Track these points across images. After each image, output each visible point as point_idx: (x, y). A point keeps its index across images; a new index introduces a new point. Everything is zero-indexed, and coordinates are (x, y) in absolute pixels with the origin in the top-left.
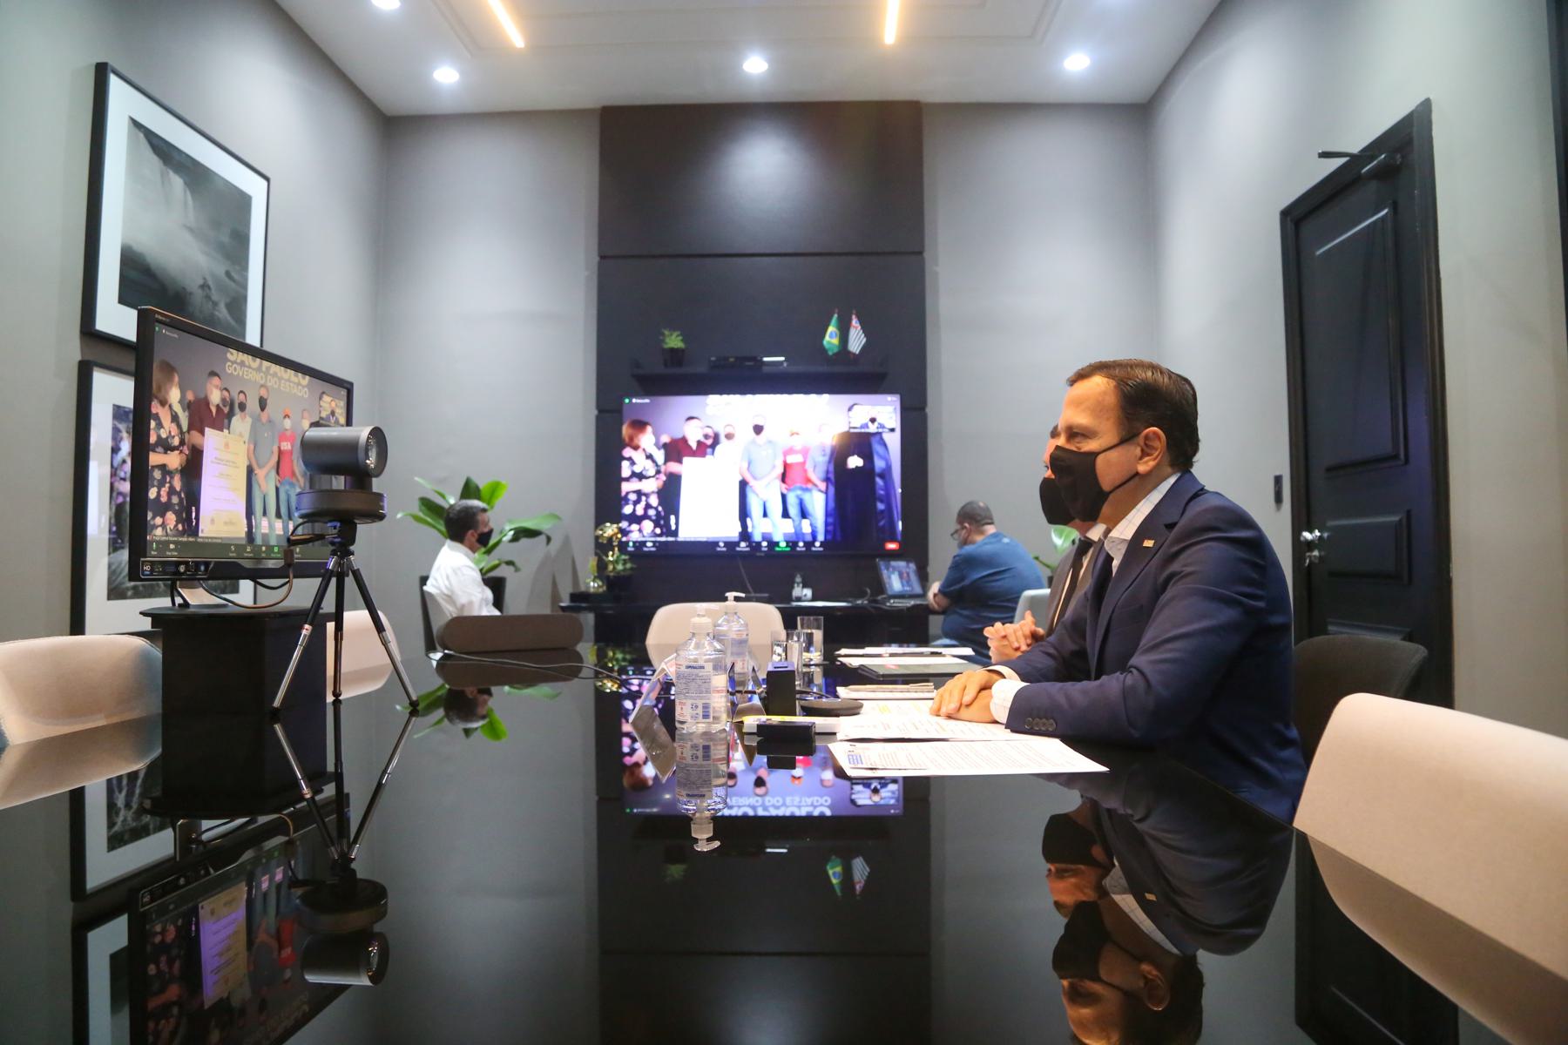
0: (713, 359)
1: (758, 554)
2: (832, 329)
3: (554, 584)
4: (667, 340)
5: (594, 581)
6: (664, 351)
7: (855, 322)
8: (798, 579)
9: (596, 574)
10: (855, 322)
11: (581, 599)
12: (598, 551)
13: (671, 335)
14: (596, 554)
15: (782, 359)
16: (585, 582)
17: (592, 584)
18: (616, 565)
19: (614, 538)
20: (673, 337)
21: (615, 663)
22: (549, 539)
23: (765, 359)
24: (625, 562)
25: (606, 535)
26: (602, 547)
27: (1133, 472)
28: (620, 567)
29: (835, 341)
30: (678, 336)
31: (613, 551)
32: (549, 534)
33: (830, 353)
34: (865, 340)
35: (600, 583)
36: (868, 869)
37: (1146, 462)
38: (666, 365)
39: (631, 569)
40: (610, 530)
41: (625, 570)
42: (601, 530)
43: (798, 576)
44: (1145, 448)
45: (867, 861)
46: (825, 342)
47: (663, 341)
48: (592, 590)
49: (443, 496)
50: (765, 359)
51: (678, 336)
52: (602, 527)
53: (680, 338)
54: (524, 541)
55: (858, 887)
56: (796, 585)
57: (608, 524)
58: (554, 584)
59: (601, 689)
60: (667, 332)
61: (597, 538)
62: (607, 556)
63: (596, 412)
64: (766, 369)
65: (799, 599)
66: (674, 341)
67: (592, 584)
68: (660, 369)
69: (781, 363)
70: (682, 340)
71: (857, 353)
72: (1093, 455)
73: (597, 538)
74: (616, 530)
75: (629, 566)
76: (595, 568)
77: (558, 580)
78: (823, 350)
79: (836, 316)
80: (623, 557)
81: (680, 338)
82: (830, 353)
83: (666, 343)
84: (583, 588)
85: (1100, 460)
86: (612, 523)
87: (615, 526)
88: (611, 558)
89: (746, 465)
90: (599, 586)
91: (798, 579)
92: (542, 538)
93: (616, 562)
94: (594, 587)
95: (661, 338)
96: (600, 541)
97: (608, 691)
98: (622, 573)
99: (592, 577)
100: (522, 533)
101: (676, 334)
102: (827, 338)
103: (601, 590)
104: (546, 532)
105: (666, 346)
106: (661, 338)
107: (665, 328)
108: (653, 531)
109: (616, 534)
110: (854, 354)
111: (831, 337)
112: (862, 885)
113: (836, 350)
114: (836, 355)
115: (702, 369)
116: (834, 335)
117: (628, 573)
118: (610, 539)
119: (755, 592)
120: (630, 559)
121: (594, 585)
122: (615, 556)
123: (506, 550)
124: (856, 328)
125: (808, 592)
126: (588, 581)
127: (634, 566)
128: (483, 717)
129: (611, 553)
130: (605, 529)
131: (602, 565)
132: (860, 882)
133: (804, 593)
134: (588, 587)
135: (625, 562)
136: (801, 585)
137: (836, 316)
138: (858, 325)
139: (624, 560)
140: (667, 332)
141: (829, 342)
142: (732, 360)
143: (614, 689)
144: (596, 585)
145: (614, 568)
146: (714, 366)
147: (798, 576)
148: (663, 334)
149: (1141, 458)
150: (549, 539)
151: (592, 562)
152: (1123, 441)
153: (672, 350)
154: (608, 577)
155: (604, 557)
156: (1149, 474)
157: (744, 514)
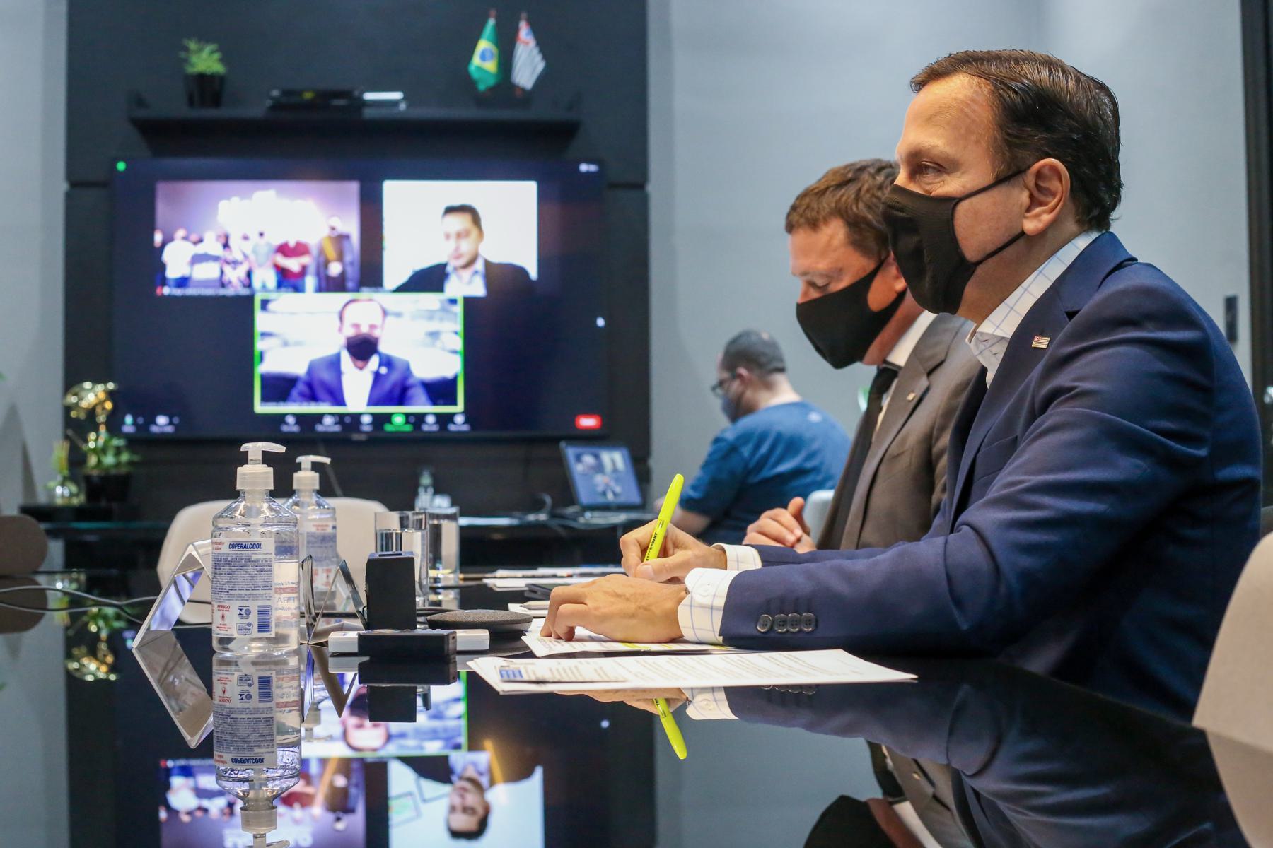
1: (356, 437)
2: (484, 45)
4: (194, 59)
5: (63, 485)
7: (524, 32)
9: (66, 472)
10: (524, 32)
12: (70, 432)
14: (67, 437)
16: (45, 487)
17: (59, 490)
21: (101, 623)
23: (369, 96)
24: (118, 451)
25: (84, 404)
29: (491, 66)
30: (212, 52)
31: (97, 430)
33: (482, 87)
39: (131, 463)
41: (118, 465)
48: (59, 502)
50: (369, 96)
52: (76, 389)
57: (87, 385)
59: (77, 675)
60: (193, 45)
61: (68, 409)
62: (86, 441)
64: (368, 113)
66: (206, 61)
67: (59, 490)
73: (68, 409)
76: (65, 463)
78: (469, 82)
79: (491, 23)
80: (117, 442)
81: (217, 56)
82: (482, 87)
83: (193, 65)
84: (42, 499)
86: (96, 381)
88: (92, 445)
90: (72, 495)
93: (102, 451)
96: (73, 414)
97: (90, 678)
98: (113, 472)
99: (60, 478)
102: (476, 60)
103: (75, 501)
107: (189, 38)
109: (102, 403)
110: (523, 90)
111: (483, 57)
113: (491, 82)
114: (492, 89)
116: (488, 54)
117: (124, 470)
121: (62, 493)
122: (101, 441)
124: (527, 43)
126: (51, 484)
127: (136, 458)
129: (92, 436)
130: (83, 394)
131: (76, 459)
134: (51, 493)
135: (118, 451)
137: (491, 23)
140: (193, 45)
141: (479, 69)
143: (102, 675)
144: (67, 493)
145: (99, 462)
151: (60, 451)
153: (202, 78)
154: (88, 479)
155: (79, 443)
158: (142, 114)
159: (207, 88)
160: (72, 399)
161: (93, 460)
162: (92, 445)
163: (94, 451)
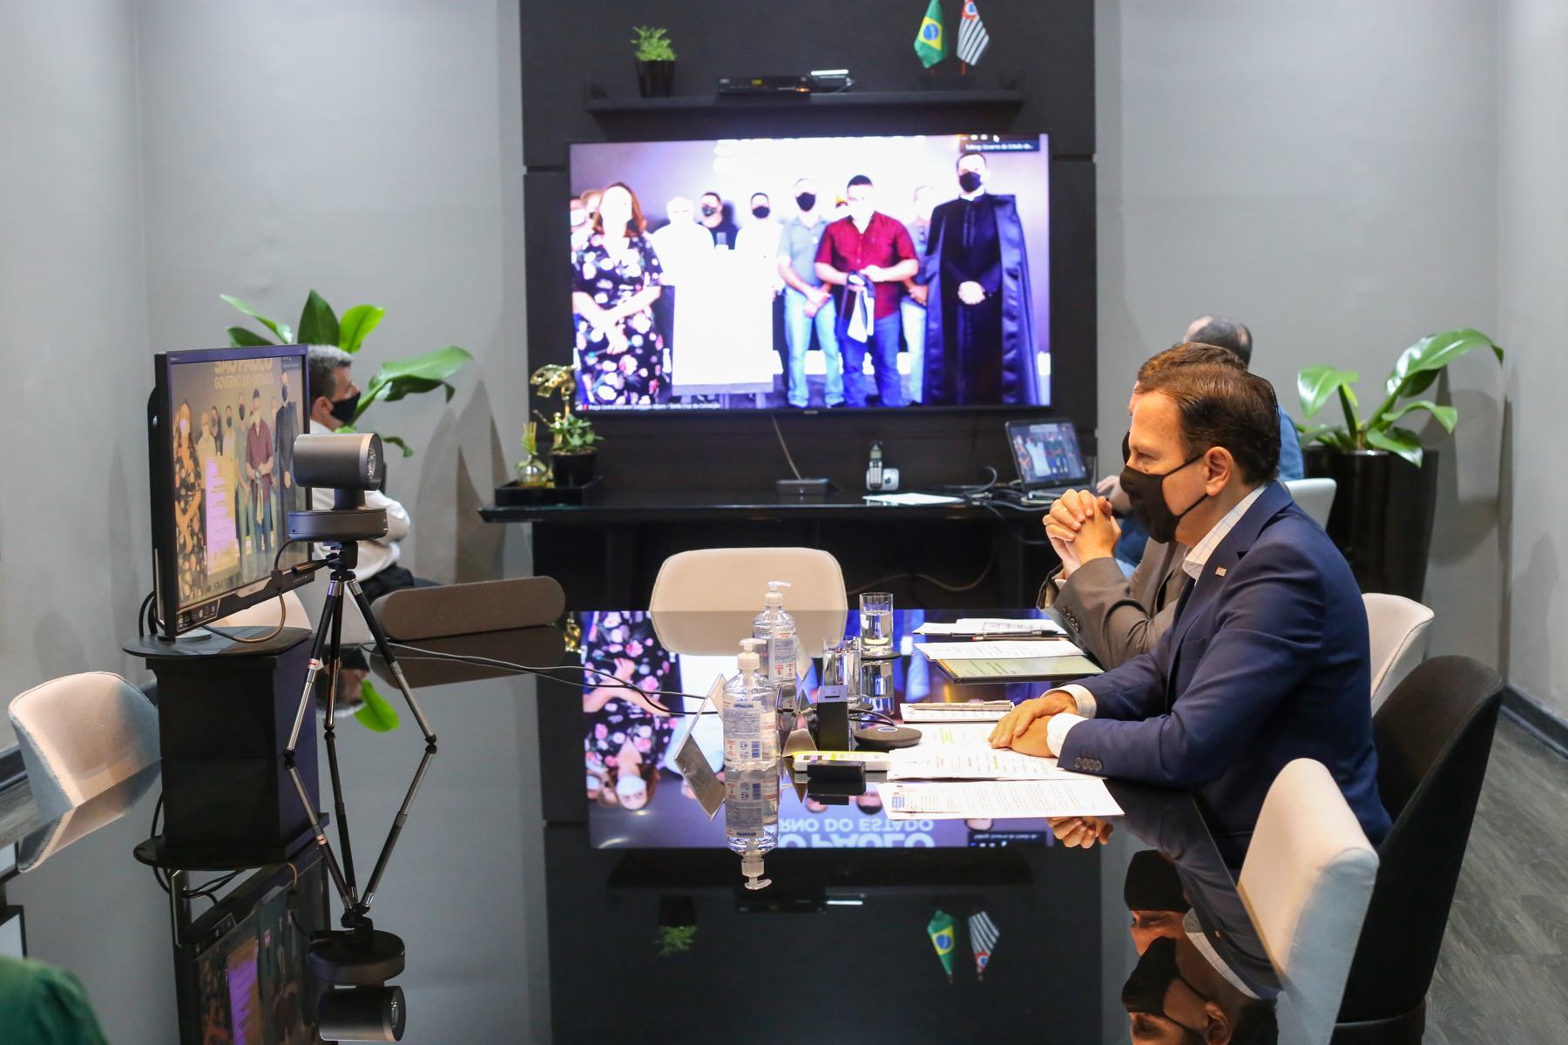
0: (724, 81)
3: (462, 466)
4: (645, 46)
5: (531, 464)
6: (638, 63)
8: (876, 454)
11: (514, 499)
12: (536, 412)
13: (651, 37)
14: (533, 418)
15: (845, 72)
18: (568, 436)
19: (563, 390)
20: (654, 41)
22: (450, 392)
26: (543, 405)
27: (1204, 493)
28: (576, 441)
29: (936, 43)
30: (661, 38)
32: (453, 384)
33: (927, 65)
34: (986, 39)
35: (543, 468)
36: (997, 933)
37: (1216, 482)
38: (644, 94)
39: (595, 443)
40: (555, 376)
41: (585, 443)
42: (541, 375)
43: (876, 448)
44: (1213, 468)
45: (995, 919)
46: (917, 45)
47: (637, 47)
49: (274, 329)
50: (814, 73)
51: (661, 38)
53: (666, 42)
54: (411, 398)
55: (979, 962)
56: (871, 464)
58: (462, 466)
60: (643, 33)
61: (533, 389)
63: (523, 170)
65: (877, 490)
66: (656, 48)
68: (630, 98)
69: (842, 81)
70: (670, 46)
71: (973, 63)
72: (1159, 478)
74: (565, 377)
75: (590, 438)
77: (467, 461)
78: (915, 60)
80: (580, 423)
81: (666, 42)
82: (927, 65)
84: (512, 476)
85: (1166, 481)
87: (565, 368)
88: (557, 425)
89: (786, 260)
91: (876, 454)
92: (441, 391)
94: (532, 475)
95: (634, 42)
100: (405, 386)
101: (659, 33)
102: (921, 37)
104: (446, 381)
105: (644, 57)
106: (634, 42)
108: (635, 372)
110: (968, 65)
111: (928, 36)
112: (986, 957)
113: (936, 59)
114: (935, 67)
115: (707, 100)
118: (557, 390)
119: (803, 477)
120: (591, 427)
121: (531, 472)
123: (381, 416)
124: (971, 18)
125: (892, 475)
126: (522, 464)
128: (356, 702)
131: (544, 438)
132: (984, 953)
133: (886, 477)
135: (583, 434)
136: (880, 464)
138: (975, 13)
139: (583, 429)
141: (923, 45)
142: (758, 82)
145: (565, 442)
146: (726, 95)
147: (876, 448)
148: (638, 37)
149: (1209, 479)
150: (450, 392)
151: (528, 433)
152: (1189, 462)
153: (653, 64)
154: (556, 458)
156: (1216, 497)
157: (781, 343)
158: (599, 104)
159: (658, 76)
160: (537, 380)
161: (559, 439)
162: (557, 425)
163: (561, 431)
